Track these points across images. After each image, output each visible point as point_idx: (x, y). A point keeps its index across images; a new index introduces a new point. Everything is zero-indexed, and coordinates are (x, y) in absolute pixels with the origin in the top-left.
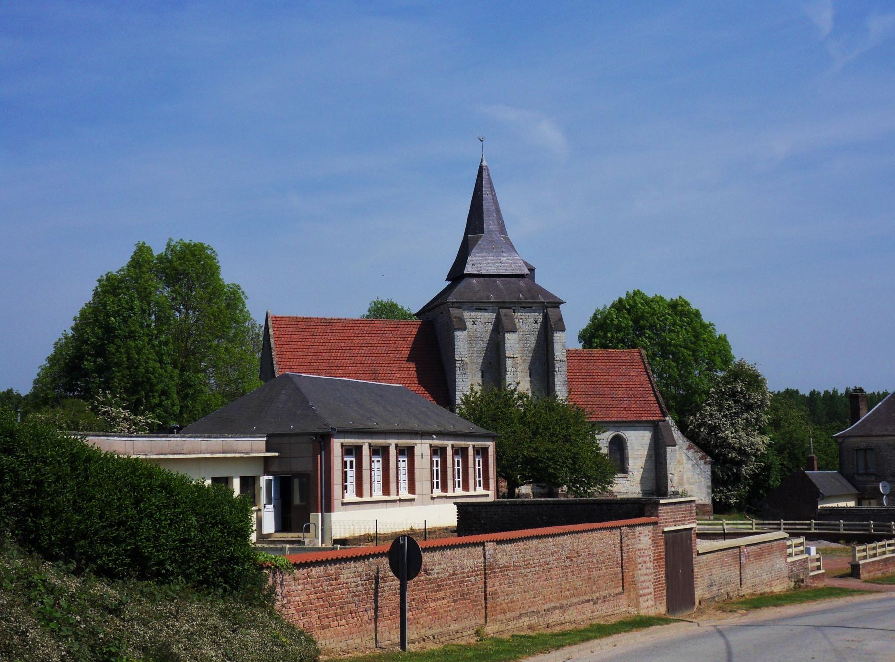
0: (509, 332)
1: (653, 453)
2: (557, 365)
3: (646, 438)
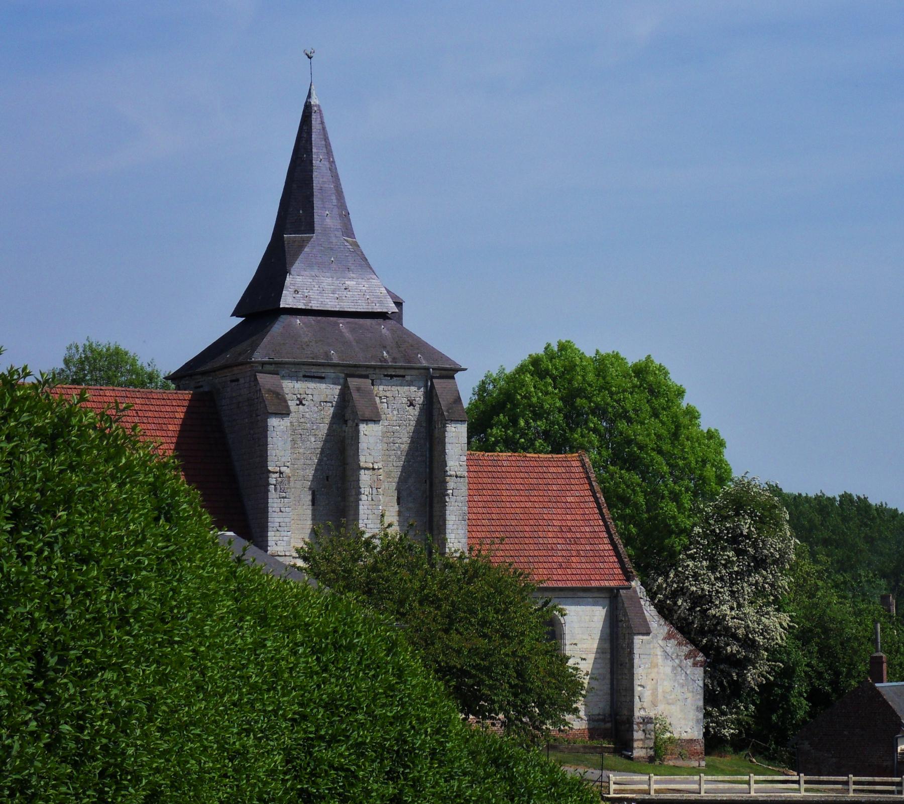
0: (367, 421)
1: (607, 646)
2: (451, 484)
3: (595, 619)
